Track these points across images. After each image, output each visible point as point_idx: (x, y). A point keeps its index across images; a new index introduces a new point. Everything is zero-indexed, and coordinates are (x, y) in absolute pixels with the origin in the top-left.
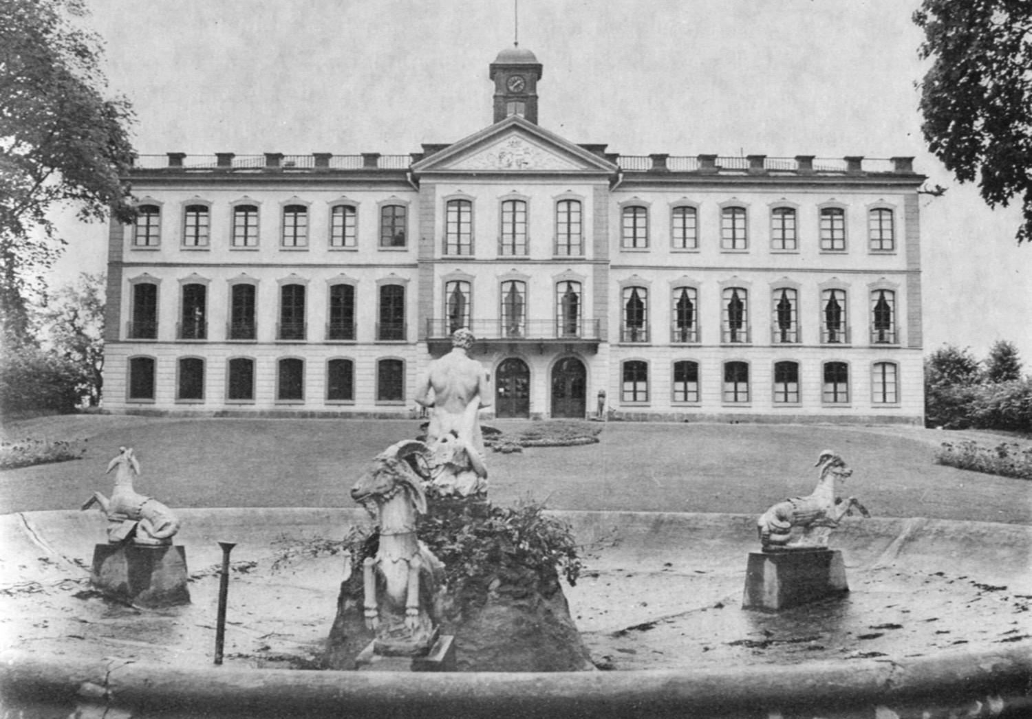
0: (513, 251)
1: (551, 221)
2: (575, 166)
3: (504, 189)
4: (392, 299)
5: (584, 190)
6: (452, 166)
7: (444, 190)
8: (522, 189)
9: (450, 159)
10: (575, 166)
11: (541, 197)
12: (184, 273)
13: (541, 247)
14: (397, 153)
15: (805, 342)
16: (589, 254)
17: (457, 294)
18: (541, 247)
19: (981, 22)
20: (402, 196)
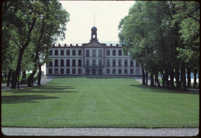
0: (94, 56)
1: (98, 53)
2: (101, 46)
3: (93, 49)
4: (80, 61)
5: (102, 49)
6: (87, 46)
7: (86, 49)
8: (95, 49)
9: (87, 45)
10: (101, 46)
11: (97, 50)
12: (55, 58)
13: (97, 55)
14: (80, 45)
15: (128, 66)
16: (103, 56)
17: (88, 61)
18: (97, 55)
19: (153, 51)
20: (81, 49)
